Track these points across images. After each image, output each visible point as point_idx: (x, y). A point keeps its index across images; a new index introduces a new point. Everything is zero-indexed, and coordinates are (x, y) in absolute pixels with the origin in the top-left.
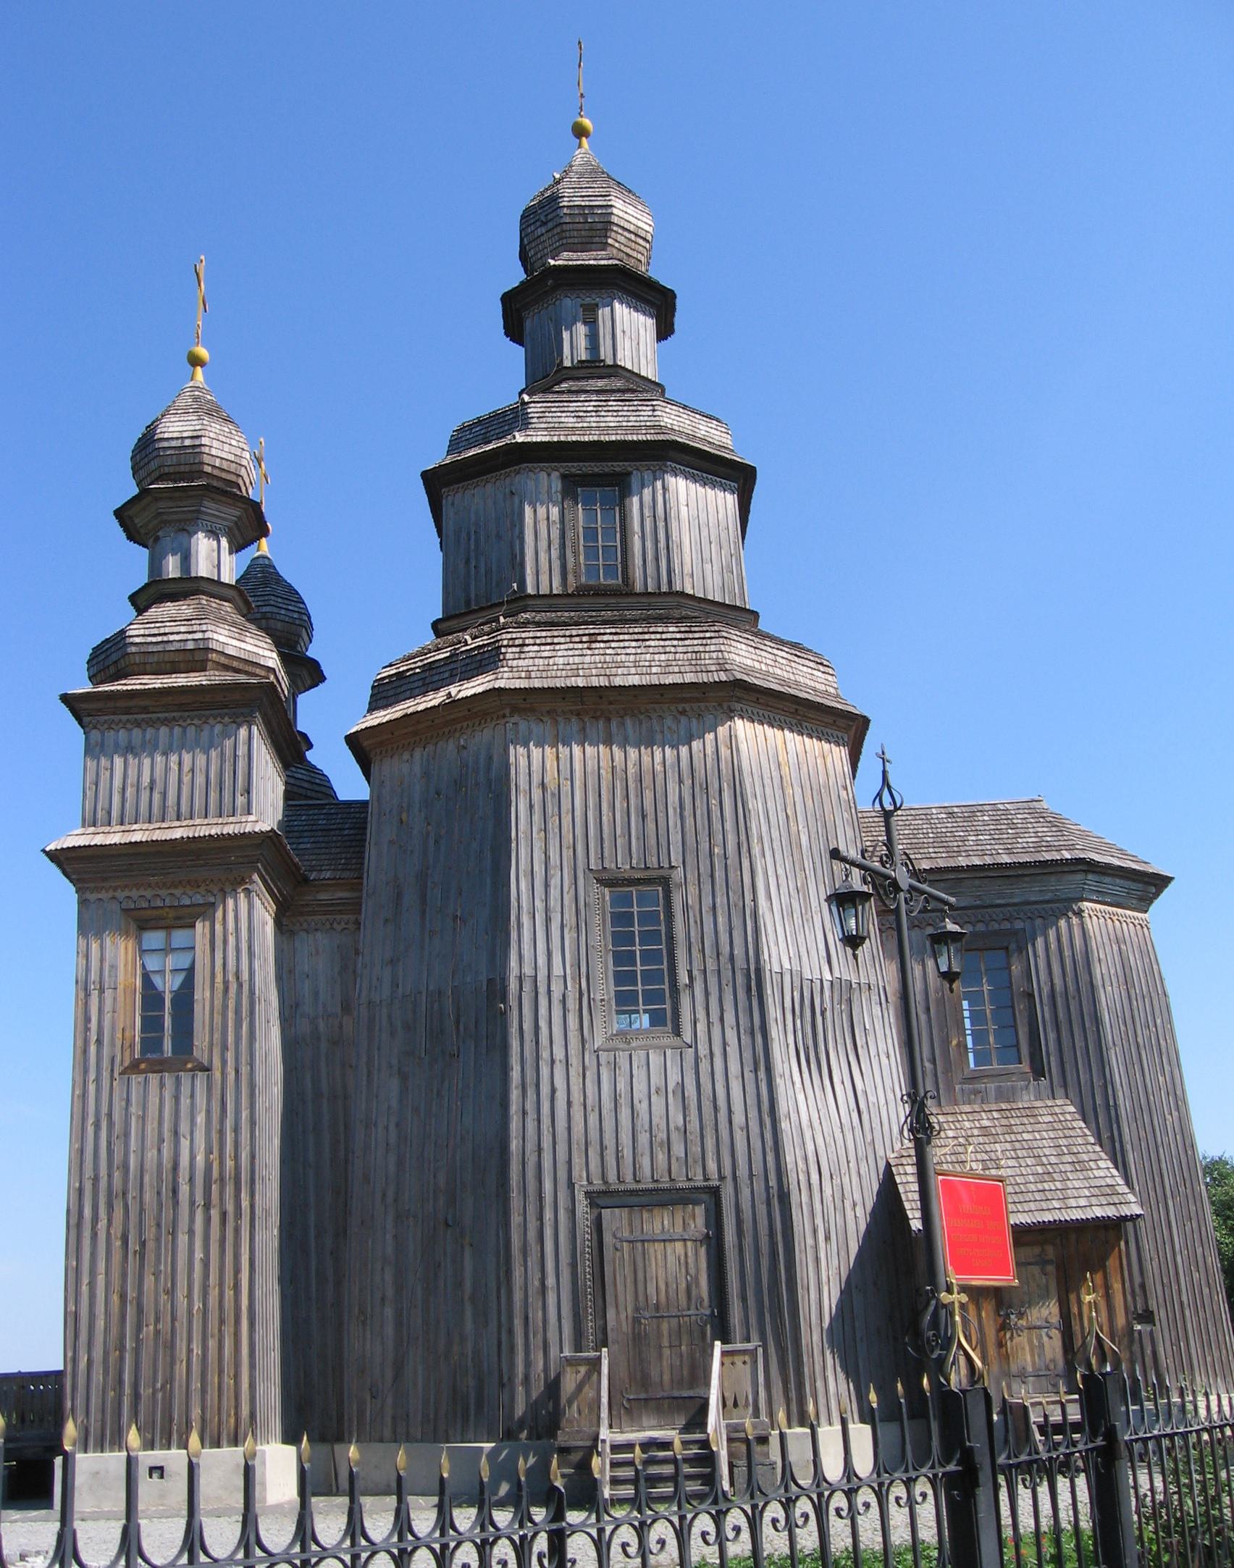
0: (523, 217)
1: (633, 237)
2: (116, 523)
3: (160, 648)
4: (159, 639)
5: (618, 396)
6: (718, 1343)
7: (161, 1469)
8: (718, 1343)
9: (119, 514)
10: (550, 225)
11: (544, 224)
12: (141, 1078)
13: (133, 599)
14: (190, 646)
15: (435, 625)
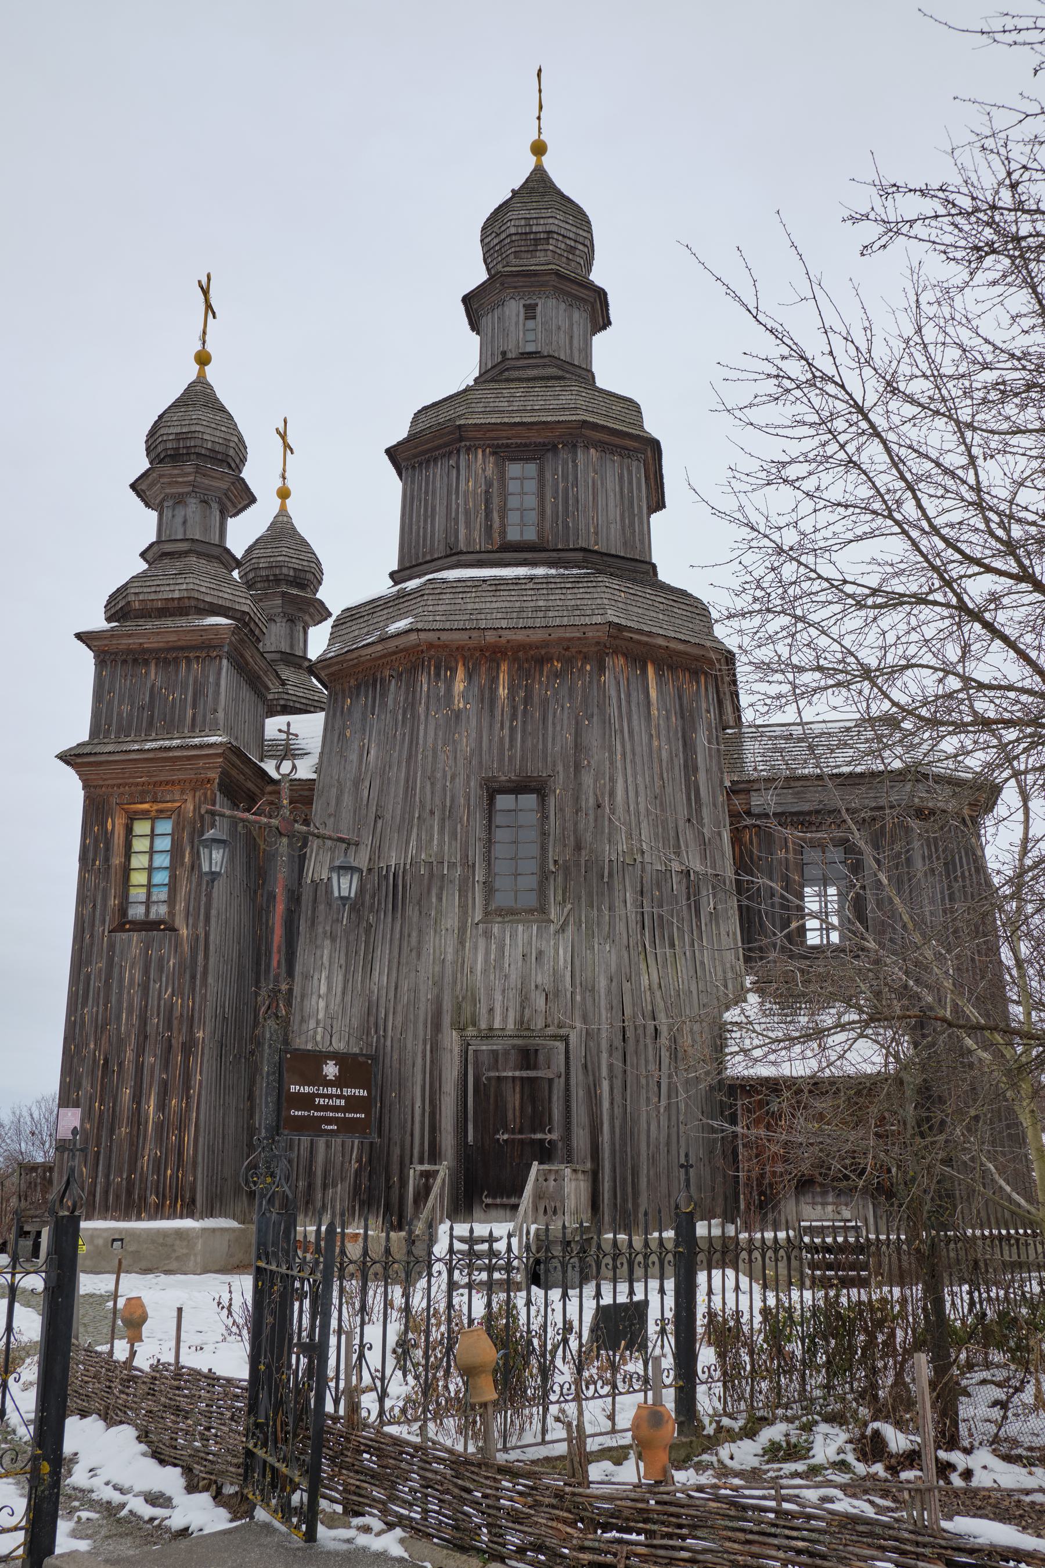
0: (483, 229)
1: (572, 244)
2: (133, 494)
3: (153, 597)
4: (153, 589)
5: (542, 383)
6: (535, 1163)
7: (122, 1240)
8: (535, 1163)
9: (133, 486)
10: (503, 236)
11: (498, 235)
12: (124, 936)
13: (143, 555)
14: (176, 595)
15: (392, 575)
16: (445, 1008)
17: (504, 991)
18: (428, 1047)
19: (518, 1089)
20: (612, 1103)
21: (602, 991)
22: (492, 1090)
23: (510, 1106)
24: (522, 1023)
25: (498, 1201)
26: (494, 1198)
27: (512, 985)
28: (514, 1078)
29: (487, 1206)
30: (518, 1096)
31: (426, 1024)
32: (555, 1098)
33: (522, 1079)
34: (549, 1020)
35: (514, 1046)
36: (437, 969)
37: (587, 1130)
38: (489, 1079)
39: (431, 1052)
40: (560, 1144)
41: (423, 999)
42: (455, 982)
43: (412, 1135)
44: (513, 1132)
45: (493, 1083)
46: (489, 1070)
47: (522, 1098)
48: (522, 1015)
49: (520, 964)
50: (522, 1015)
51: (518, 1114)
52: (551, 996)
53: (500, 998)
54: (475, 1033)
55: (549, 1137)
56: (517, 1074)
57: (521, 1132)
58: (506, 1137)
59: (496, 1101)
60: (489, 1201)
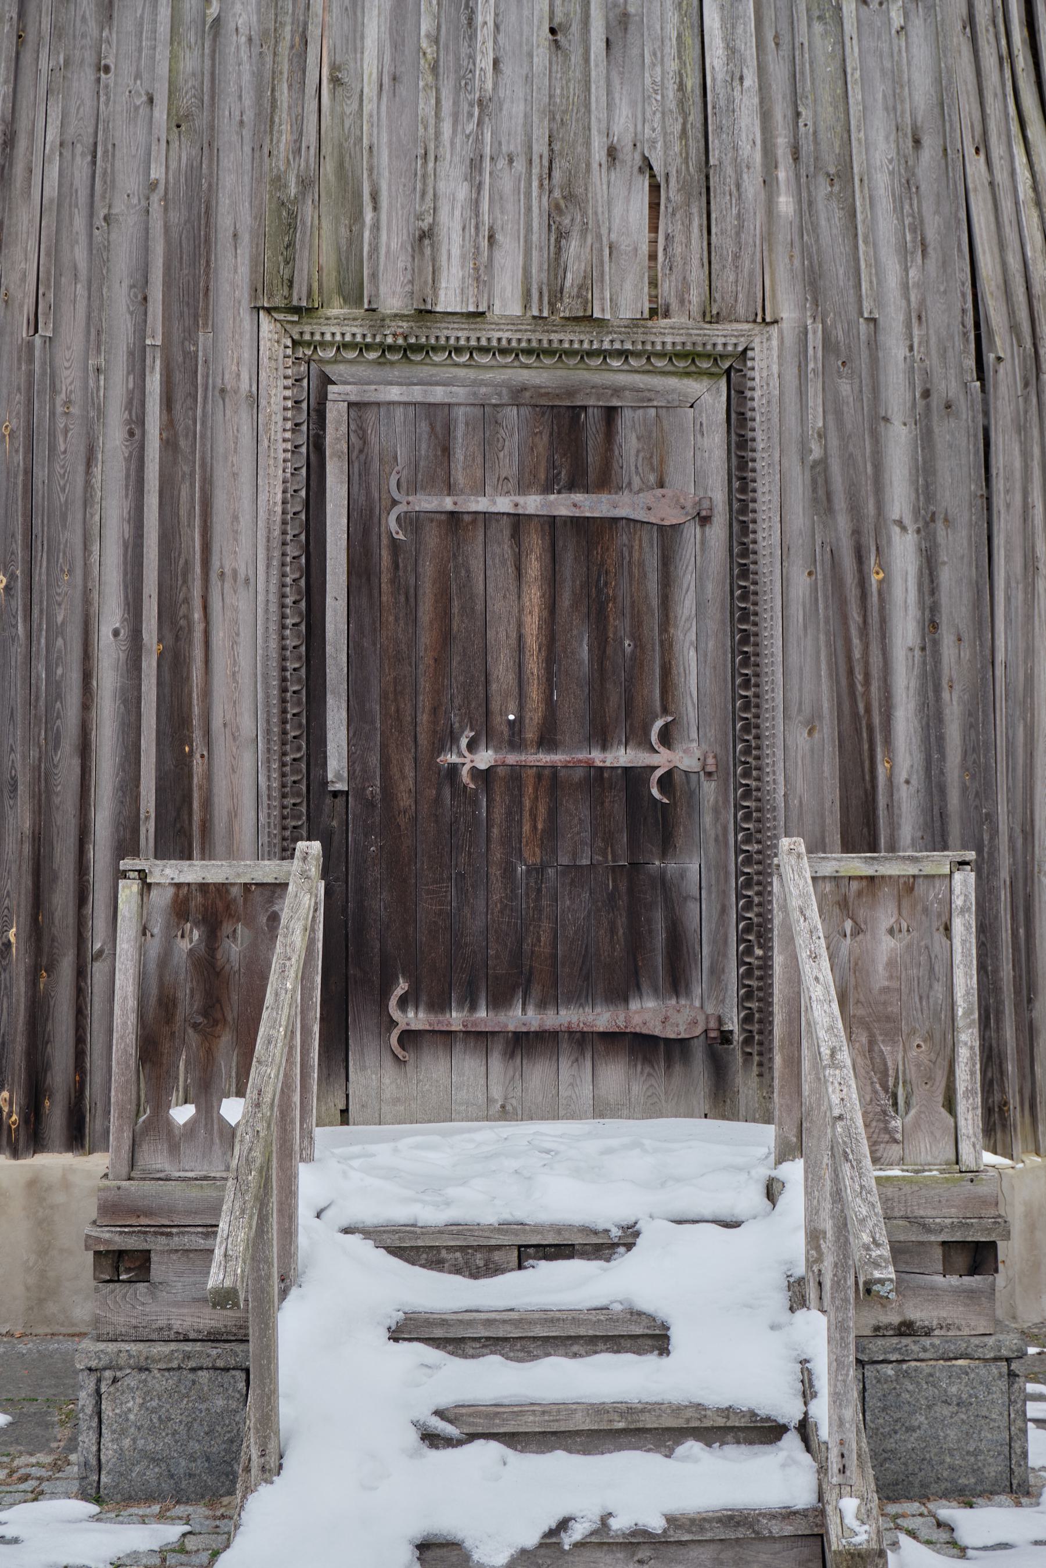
16: (224, 221)
17: (475, 164)
18: (154, 383)
19: (534, 568)
20: (931, 624)
21: (882, 181)
22: (428, 569)
23: (501, 635)
24: (556, 294)
25: (456, 1019)
26: (440, 1004)
27: (514, 144)
28: (518, 522)
29: (410, 1038)
30: (534, 595)
31: (143, 281)
32: (686, 606)
33: (552, 521)
34: (667, 289)
35: (517, 393)
36: (189, 63)
37: (827, 730)
38: (413, 522)
39: (168, 402)
40: (709, 790)
41: (129, 182)
42: (266, 117)
43: (85, 749)
44: (515, 740)
45: (432, 538)
46: (414, 487)
47: (552, 607)
48: (556, 264)
49: (542, 55)
50: (556, 264)
51: (534, 666)
52: (671, 194)
53: (462, 192)
54: (356, 331)
55: (663, 759)
56: (533, 503)
57: (547, 741)
58: (484, 759)
59: (444, 615)
60: (416, 1019)
